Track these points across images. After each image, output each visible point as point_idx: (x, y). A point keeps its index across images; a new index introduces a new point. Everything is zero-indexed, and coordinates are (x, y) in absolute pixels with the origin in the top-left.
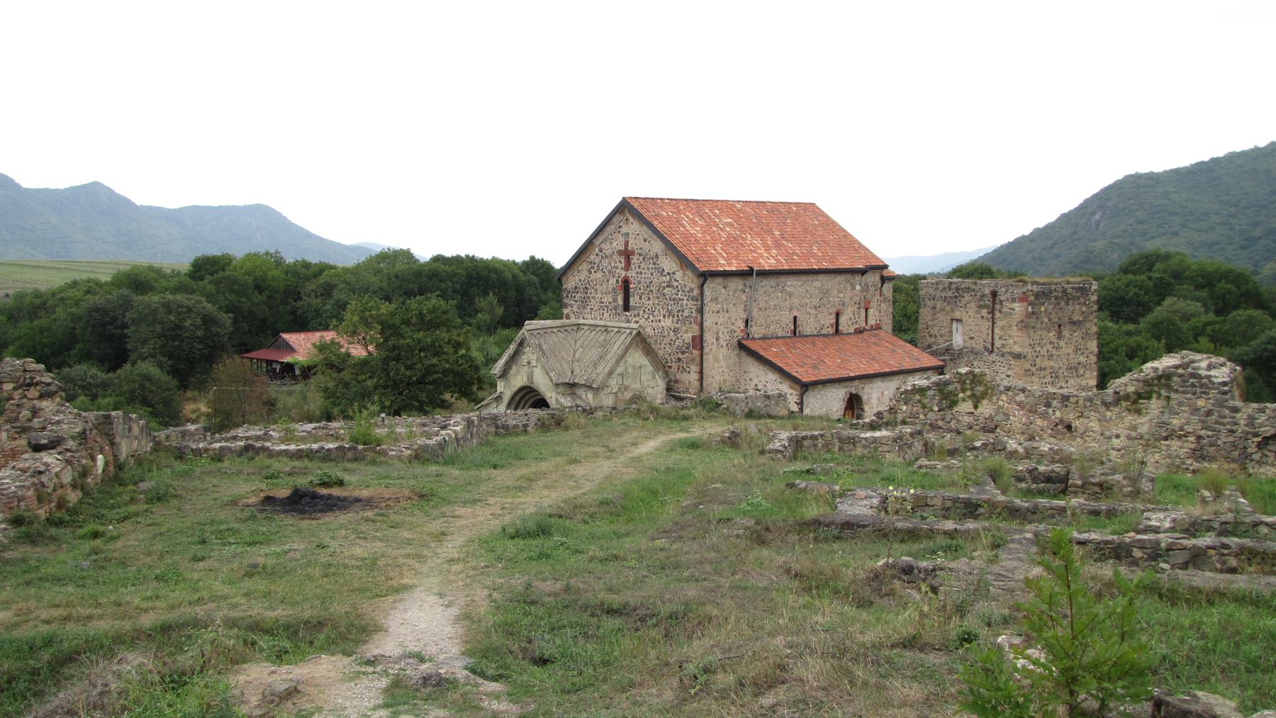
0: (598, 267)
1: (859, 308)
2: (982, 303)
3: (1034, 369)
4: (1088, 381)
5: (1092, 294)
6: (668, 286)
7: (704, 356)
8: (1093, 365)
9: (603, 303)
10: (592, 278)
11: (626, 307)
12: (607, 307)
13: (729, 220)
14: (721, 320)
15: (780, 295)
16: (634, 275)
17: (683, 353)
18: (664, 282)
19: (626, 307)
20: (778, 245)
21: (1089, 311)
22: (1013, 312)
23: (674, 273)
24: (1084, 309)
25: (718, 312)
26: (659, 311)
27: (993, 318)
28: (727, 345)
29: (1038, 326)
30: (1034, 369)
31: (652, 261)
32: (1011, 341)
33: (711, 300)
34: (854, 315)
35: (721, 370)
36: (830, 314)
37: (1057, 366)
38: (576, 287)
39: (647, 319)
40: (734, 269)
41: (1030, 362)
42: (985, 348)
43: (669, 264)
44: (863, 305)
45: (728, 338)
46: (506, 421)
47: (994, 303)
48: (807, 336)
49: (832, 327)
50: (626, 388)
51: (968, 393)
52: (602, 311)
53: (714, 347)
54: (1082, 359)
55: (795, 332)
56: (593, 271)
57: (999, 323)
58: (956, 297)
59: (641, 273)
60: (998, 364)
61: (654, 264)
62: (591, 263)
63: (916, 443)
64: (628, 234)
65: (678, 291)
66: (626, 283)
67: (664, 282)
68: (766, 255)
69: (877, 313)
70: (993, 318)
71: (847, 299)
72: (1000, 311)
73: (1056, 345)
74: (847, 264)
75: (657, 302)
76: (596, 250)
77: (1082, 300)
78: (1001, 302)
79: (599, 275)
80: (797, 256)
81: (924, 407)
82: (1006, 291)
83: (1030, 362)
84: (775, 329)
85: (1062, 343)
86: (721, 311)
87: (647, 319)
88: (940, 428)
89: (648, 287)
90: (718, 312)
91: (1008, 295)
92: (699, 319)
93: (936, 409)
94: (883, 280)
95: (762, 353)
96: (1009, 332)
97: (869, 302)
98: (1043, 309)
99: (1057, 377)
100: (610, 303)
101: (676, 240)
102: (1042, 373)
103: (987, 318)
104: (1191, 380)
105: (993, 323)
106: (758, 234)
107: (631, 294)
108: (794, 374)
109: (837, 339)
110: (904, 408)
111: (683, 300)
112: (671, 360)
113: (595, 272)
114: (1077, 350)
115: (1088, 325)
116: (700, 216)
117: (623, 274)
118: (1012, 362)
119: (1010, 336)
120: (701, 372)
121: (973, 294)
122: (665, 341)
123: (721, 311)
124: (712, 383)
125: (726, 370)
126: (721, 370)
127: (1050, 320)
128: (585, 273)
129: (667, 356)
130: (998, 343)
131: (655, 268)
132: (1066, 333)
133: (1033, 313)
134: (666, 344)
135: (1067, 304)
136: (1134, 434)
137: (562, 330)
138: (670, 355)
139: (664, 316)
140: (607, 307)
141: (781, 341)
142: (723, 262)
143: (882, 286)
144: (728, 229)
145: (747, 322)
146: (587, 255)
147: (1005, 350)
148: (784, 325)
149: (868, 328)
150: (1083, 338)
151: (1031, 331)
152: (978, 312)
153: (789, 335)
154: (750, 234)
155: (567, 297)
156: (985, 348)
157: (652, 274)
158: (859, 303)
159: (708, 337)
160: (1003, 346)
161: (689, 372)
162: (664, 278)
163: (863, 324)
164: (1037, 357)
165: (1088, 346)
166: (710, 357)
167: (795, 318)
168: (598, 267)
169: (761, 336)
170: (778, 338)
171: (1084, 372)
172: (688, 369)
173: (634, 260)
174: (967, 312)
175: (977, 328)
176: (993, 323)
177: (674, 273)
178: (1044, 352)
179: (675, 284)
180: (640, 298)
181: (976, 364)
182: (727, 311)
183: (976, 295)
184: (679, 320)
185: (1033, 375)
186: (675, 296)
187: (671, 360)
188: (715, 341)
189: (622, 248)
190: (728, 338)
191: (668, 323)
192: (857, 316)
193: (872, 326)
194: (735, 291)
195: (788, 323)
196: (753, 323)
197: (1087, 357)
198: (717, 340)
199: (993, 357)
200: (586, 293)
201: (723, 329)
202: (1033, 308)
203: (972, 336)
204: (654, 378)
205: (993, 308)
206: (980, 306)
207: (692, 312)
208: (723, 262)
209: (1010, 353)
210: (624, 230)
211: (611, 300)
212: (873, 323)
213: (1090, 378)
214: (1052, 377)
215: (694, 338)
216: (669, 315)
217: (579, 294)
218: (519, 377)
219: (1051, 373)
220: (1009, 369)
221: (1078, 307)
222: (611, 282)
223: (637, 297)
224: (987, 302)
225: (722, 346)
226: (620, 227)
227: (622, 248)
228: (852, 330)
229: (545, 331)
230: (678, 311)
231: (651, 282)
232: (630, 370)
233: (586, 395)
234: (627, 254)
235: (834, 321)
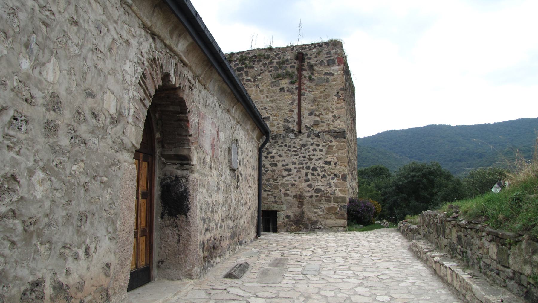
2: (280, 71)
22: (331, 78)
27: (299, 89)
32: (330, 116)
42: (288, 130)
47: (300, 69)
57: (309, 95)
58: (242, 69)
60: (311, 148)
70: (299, 89)
72: (310, 79)
78: (311, 67)
82: (319, 53)
96: (326, 105)
103: (289, 90)
105: (300, 95)
118: (334, 143)
119: (327, 110)
121: (267, 61)
130: (307, 121)
147: (318, 130)
152: (273, 84)
156: (288, 130)
160: (316, 124)
174: (258, 86)
175: (274, 105)
176: (300, 95)
183: (271, 63)
199: (304, 139)
205: (300, 77)
206: (279, 76)
209: (329, 132)
220: (327, 153)
224: (290, 70)
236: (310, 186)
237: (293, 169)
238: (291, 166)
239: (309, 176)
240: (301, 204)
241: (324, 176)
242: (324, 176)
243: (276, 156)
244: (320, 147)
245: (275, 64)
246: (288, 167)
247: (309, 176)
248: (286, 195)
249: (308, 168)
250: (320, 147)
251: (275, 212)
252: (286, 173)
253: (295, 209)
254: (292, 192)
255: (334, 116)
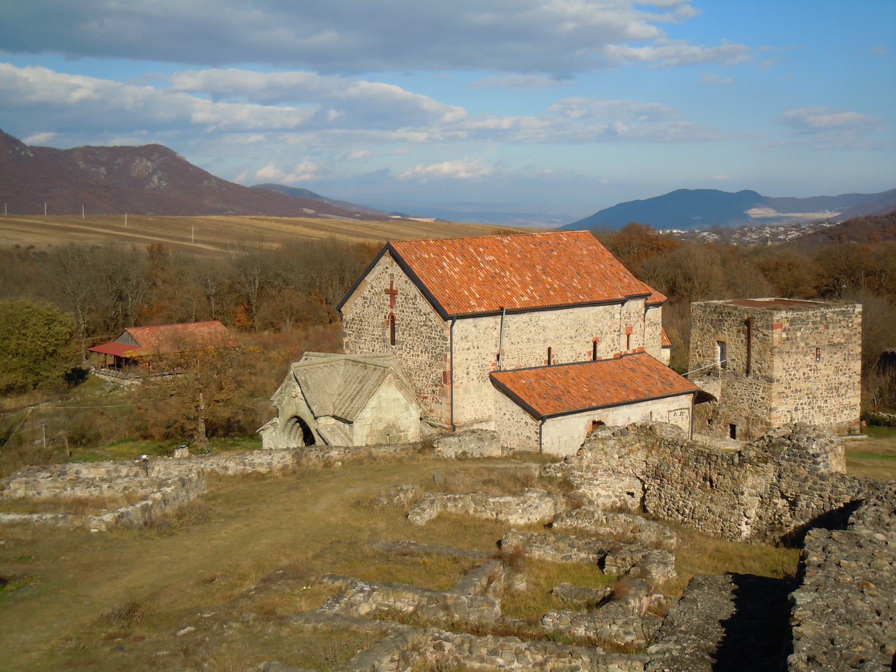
0: (370, 301)
1: (619, 336)
3: (788, 391)
4: (850, 400)
5: (856, 317)
6: (425, 325)
7: (454, 390)
8: (857, 384)
9: (374, 335)
10: (365, 312)
11: (393, 342)
12: (377, 339)
13: (491, 258)
14: (472, 356)
15: (533, 329)
16: (398, 312)
17: (436, 386)
18: (421, 321)
19: (393, 342)
20: (536, 281)
21: (852, 333)
23: (429, 314)
24: (846, 331)
25: (468, 349)
26: (418, 347)
28: (478, 378)
29: (793, 351)
30: (788, 391)
31: (411, 301)
33: (462, 338)
34: (613, 341)
35: (471, 400)
36: (587, 342)
37: (815, 388)
38: (353, 319)
39: (408, 353)
40: (484, 310)
41: (784, 385)
43: (426, 307)
44: (623, 331)
45: (479, 372)
46: (252, 460)
48: (562, 365)
49: (590, 354)
50: (380, 420)
51: (643, 443)
52: (373, 342)
53: (465, 381)
54: (843, 379)
55: (549, 361)
56: (366, 305)
58: (720, 321)
59: (403, 311)
61: (414, 304)
62: (364, 298)
63: (543, 505)
64: (392, 275)
65: (432, 330)
66: (393, 317)
67: (421, 321)
68: (521, 292)
69: (640, 338)
71: (606, 328)
73: (813, 367)
74: (605, 296)
75: (416, 338)
76: (369, 287)
77: (844, 323)
79: (371, 308)
80: (555, 290)
81: (606, 454)
83: (784, 385)
84: (528, 361)
85: (819, 365)
86: (471, 348)
87: (408, 353)
88: (620, 473)
89: (409, 324)
90: (468, 349)
91: (763, 322)
92: (449, 357)
93: (616, 456)
94: (647, 307)
95: (509, 386)
97: (631, 329)
98: (799, 334)
99: (814, 397)
100: (380, 336)
101: (432, 284)
102: (798, 395)
104: (794, 450)
106: (517, 270)
107: (396, 329)
108: (534, 407)
109: (593, 365)
110: (589, 455)
111: (436, 338)
112: (427, 391)
113: (368, 307)
114: (837, 370)
115: (850, 346)
116: (463, 256)
117: (390, 311)
120: (452, 404)
122: (422, 375)
123: (471, 348)
124: (462, 413)
125: (476, 401)
126: (471, 400)
127: (807, 344)
128: (360, 306)
129: (424, 388)
130: (754, 366)
131: (414, 308)
132: (824, 355)
133: (788, 339)
134: (423, 377)
135: (827, 328)
136: (754, 491)
137: (328, 365)
138: (426, 386)
139: (422, 352)
140: (377, 339)
141: (533, 371)
142: (473, 303)
143: (646, 311)
144: (488, 267)
145: (498, 356)
146: (362, 290)
148: (537, 357)
149: (629, 352)
150: (845, 359)
151: (785, 356)
153: (543, 365)
154: (510, 272)
155: (346, 327)
157: (412, 313)
158: (619, 331)
159: (458, 372)
161: (441, 404)
162: (421, 317)
163: (624, 349)
164: (792, 379)
165: (851, 367)
166: (461, 390)
167: (549, 349)
168: (370, 301)
169: (513, 367)
170: (530, 369)
171: (846, 391)
172: (440, 401)
173: (399, 298)
177: (429, 314)
178: (799, 374)
179: (430, 324)
180: (403, 334)
181: (736, 385)
182: (478, 348)
184: (433, 356)
185: (787, 396)
186: (429, 335)
187: (427, 391)
188: (465, 375)
189: (388, 287)
190: (479, 372)
191: (425, 357)
192: (616, 343)
193: (634, 350)
194: (486, 329)
195: (542, 353)
196: (505, 357)
197: (850, 377)
198: (468, 374)
200: (361, 325)
201: (473, 363)
202: (787, 334)
203: (734, 358)
204: (408, 409)
207: (443, 351)
208: (473, 303)
210: (390, 271)
211: (380, 333)
212: (636, 347)
213: (853, 397)
214: (809, 398)
215: (444, 373)
216: (425, 351)
217: (356, 325)
218: (290, 407)
219: (807, 394)
221: (839, 330)
222: (380, 317)
223: (401, 333)
225: (472, 380)
226: (387, 268)
227: (388, 287)
228: (611, 356)
229: (312, 366)
230: (432, 349)
231: (411, 320)
232: (384, 404)
233: (344, 427)
234: (392, 293)
235: (592, 349)
236: (753, 412)
237: (745, 399)
238: (744, 397)
239: (753, 405)
240: (748, 423)
241: (760, 407)
242: (760, 407)
243: (737, 388)
244: (759, 387)
245: (738, 322)
246: (742, 397)
247: (753, 405)
248: (741, 416)
249: (752, 399)
250: (759, 387)
251: (735, 426)
252: (742, 401)
253: (745, 425)
254: (744, 414)
255: (768, 366)
